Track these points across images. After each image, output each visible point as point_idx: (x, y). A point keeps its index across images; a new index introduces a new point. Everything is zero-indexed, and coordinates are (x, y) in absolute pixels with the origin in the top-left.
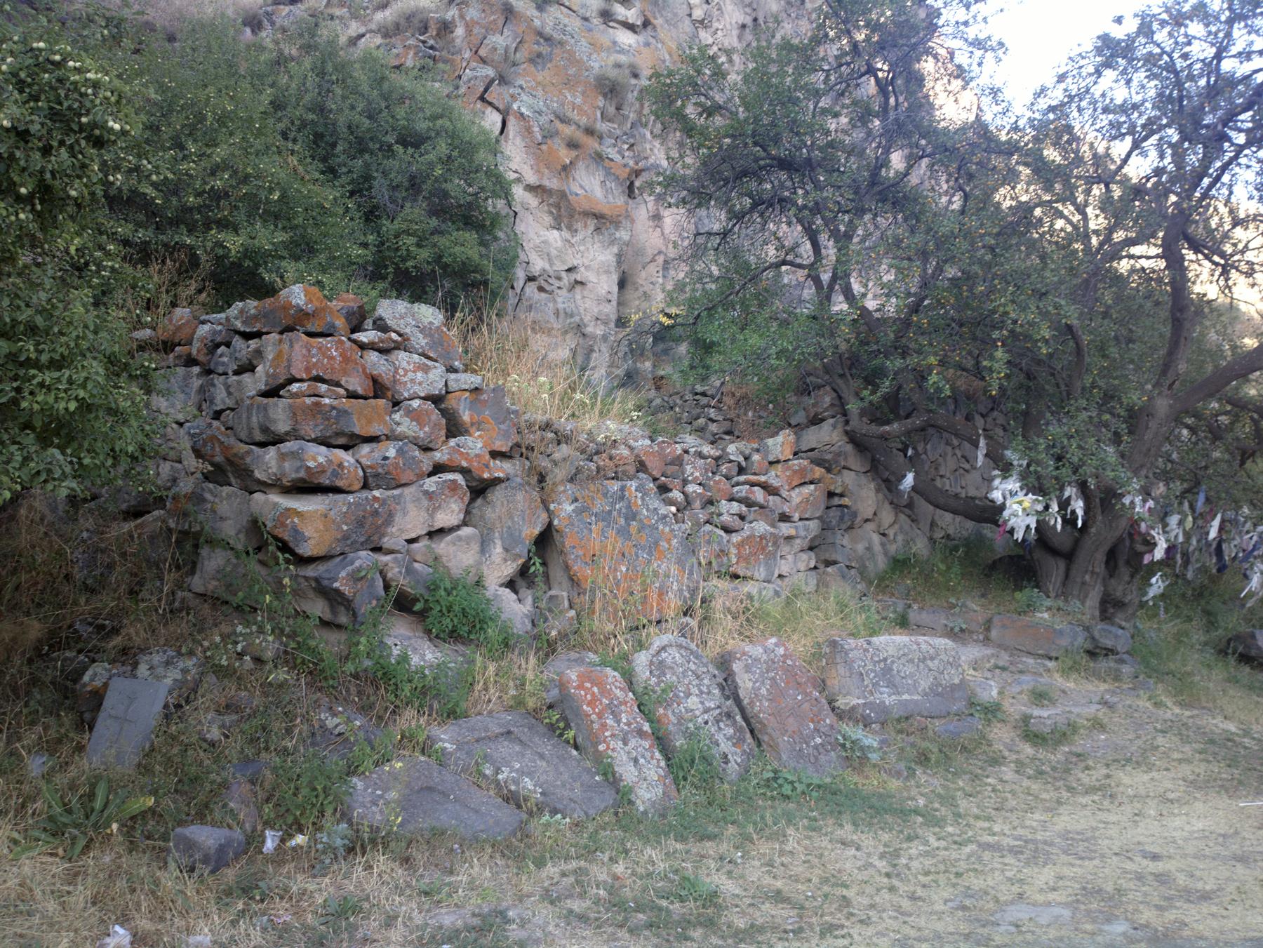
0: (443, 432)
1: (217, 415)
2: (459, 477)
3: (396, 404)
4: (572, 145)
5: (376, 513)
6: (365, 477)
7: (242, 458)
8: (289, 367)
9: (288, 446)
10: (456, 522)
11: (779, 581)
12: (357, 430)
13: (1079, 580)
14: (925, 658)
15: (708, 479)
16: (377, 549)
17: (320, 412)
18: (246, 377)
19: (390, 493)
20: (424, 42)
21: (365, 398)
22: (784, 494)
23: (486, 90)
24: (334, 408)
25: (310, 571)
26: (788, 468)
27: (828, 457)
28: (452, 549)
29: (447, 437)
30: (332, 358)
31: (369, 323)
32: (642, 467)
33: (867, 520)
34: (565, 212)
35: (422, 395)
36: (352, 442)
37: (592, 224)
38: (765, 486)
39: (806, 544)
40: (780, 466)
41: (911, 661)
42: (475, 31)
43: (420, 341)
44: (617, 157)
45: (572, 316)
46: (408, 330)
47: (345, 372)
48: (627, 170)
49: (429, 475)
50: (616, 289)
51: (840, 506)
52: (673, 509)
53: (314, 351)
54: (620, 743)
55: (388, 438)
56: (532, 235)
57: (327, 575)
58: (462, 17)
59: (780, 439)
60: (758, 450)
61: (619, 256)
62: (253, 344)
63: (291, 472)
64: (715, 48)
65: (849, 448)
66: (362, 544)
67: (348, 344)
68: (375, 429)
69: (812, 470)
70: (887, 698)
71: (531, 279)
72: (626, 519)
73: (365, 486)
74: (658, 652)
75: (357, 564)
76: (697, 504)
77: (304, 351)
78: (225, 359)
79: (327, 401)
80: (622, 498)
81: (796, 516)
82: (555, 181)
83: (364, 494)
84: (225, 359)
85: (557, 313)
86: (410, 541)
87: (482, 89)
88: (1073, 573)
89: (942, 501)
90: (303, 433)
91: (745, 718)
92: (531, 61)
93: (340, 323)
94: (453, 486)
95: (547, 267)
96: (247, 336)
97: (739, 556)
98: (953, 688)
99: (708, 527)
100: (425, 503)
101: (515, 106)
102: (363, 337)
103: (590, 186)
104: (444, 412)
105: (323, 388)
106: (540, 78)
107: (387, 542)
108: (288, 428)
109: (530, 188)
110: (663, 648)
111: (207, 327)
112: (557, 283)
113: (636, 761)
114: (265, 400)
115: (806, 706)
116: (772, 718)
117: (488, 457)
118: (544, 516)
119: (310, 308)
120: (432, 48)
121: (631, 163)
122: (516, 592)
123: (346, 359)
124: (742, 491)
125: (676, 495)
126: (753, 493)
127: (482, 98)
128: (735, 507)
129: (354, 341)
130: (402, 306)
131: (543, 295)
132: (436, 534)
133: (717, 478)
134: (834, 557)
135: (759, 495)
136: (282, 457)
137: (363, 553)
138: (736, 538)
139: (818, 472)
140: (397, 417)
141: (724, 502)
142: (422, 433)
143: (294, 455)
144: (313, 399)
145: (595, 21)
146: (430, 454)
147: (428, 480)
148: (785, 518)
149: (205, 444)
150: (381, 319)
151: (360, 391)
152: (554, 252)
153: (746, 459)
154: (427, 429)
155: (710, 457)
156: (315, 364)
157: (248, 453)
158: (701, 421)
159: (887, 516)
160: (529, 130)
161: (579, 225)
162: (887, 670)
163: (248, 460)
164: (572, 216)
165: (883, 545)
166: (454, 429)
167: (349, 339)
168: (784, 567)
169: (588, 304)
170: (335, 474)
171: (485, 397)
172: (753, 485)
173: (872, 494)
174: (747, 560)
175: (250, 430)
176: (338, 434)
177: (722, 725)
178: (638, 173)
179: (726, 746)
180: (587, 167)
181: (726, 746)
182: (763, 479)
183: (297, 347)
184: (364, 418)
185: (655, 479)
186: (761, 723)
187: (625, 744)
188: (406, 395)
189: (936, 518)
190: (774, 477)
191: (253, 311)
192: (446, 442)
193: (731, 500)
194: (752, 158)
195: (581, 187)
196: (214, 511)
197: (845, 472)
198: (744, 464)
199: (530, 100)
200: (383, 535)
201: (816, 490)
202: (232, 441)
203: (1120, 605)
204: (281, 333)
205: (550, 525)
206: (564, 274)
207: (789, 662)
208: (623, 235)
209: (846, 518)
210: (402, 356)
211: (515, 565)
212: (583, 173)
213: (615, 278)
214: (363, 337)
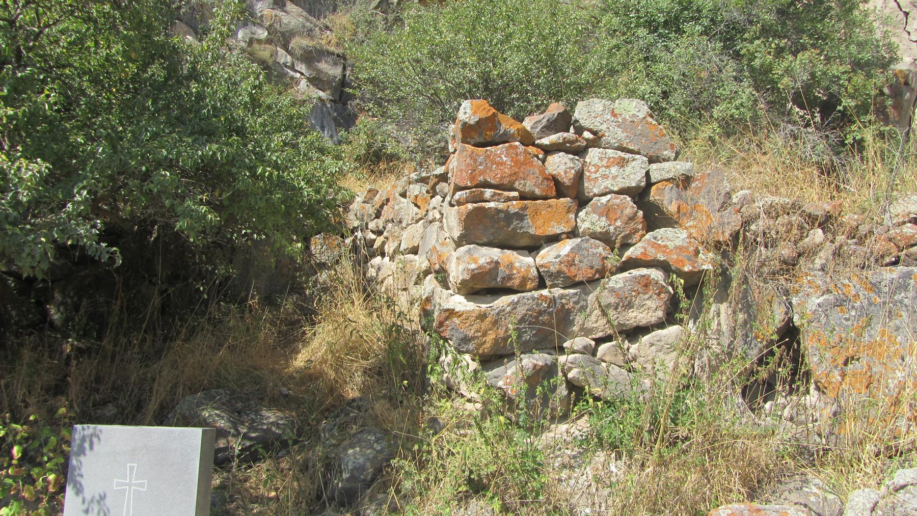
2: (656, 274)
3: (582, 201)
10: (653, 320)
21: (545, 198)
30: (503, 163)
35: (616, 189)
43: (614, 134)
46: (604, 127)
68: (557, 229)
73: (542, 285)
79: (492, 205)
83: (536, 294)
94: (646, 283)
105: (488, 193)
132: (634, 333)
151: (537, 192)
154: (618, 223)
156: (482, 173)
188: (596, 191)
210: (593, 154)
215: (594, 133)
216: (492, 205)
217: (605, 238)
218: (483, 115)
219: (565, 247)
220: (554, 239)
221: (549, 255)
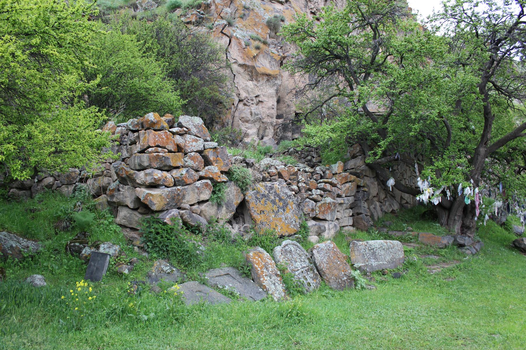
0: (203, 164)
1: (123, 160)
2: (209, 182)
4: (258, 48)
5: (178, 195)
6: (175, 182)
7: (132, 175)
8: (148, 142)
9: (148, 171)
11: (337, 221)
12: (172, 164)
13: (453, 218)
14: (389, 248)
15: (308, 180)
16: (179, 208)
17: (158, 158)
18: (133, 146)
19: (183, 187)
20: (199, 12)
21: (174, 152)
22: (339, 186)
23: (223, 29)
24: (163, 156)
25: (156, 216)
27: (359, 171)
28: (207, 209)
29: (205, 166)
30: (163, 138)
31: (176, 124)
32: (280, 175)
33: (374, 197)
34: (253, 73)
35: (195, 150)
36: (170, 169)
37: (265, 78)
38: (331, 184)
39: (348, 206)
41: (384, 249)
42: (219, 7)
43: (194, 130)
44: (276, 52)
45: (257, 115)
47: (167, 144)
48: (280, 57)
49: (198, 180)
50: (276, 104)
52: (294, 193)
53: (157, 136)
54: (269, 278)
55: (183, 167)
56: (241, 83)
57: (162, 217)
59: (337, 164)
60: (328, 169)
61: (277, 91)
62: (136, 134)
63: (149, 180)
64: (315, 9)
65: (367, 168)
66: (174, 206)
67: (169, 133)
68: (179, 164)
69: (351, 177)
70: (374, 263)
73: (175, 185)
74: (285, 247)
75: (172, 213)
76: (303, 191)
77: (153, 137)
78: (126, 140)
79: (161, 154)
81: (344, 195)
82: (250, 62)
83: (174, 188)
84: (126, 140)
85: (251, 114)
86: (191, 205)
87: (221, 29)
88: (451, 216)
89: (402, 188)
90: (153, 166)
91: (318, 271)
92: (242, 18)
93: (166, 125)
94: (207, 185)
95: (247, 95)
96: (134, 132)
97: (320, 211)
99: (308, 200)
100: (196, 191)
101: (235, 35)
102: (174, 130)
103: (264, 65)
105: (160, 149)
107: (183, 205)
108: (148, 164)
109: (240, 65)
110: (287, 245)
111: (120, 128)
112: (251, 102)
113: (274, 284)
114: (140, 154)
115: (341, 266)
116: (328, 270)
117: (220, 173)
118: (242, 195)
119: (155, 121)
120: (202, 14)
121: (282, 54)
122: (232, 225)
123: (168, 139)
124: (322, 185)
126: (326, 186)
127: (222, 32)
130: (188, 118)
131: (246, 107)
132: (200, 203)
133: (312, 180)
134: (360, 212)
135: (328, 187)
136: (146, 175)
137: (174, 210)
138: (319, 204)
139: (353, 177)
140: (186, 159)
141: (314, 190)
142: (195, 165)
143: (150, 174)
144: (156, 154)
146: (198, 173)
147: (197, 182)
148: (339, 196)
149: (120, 171)
150: (180, 123)
151: (173, 150)
152: (250, 90)
153: (324, 173)
154: (197, 163)
155: (309, 172)
157: (134, 173)
158: (309, 158)
160: (240, 43)
161: (260, 79)
162: (374, 253)
163: (134, 176)
164: (257, 76)
165: (381, 206)
166: (207, 162)
167: (169, 131)
168: (339, 215)
169: (265, 110)
170: (164, 180)
171: (219, 150)
172: (326, 183)
174: (323, 213)
175: (135, 165)
176: (165, 166)
177: (309, 273)
178: (284, 58)
179: (310, 280)
180: (263, 56)
181: (310, 280)
182: (330, 180)
183: (151, 135)
184: (174, 160)
185: (286, 181)
186: (323, 272)
187: (271, 278)
188: (189, 151)
189: (403, 196)
190: (334, 180)
191: (136, 123)
192: (203, 168)
193: (317, 189)
196: (123, 194)
197: (365, 178)
198: (323, 175)
199: (241, 32)
200: (182, 203)
202: (129, 169)
203: (468, 228)
204: (145, 130)
205: (244, 199)
206: (254, 98)
207: (335, 250)
208: (278, 82)
209: (365, 196)
210: (188, 136)
212: (262, 59)
213: (275, 99)
214: (174, 130)
216: (161, 154)
217: (192, 168)
219: (184, 171)
220: (178, 168)
221: (175, 173)
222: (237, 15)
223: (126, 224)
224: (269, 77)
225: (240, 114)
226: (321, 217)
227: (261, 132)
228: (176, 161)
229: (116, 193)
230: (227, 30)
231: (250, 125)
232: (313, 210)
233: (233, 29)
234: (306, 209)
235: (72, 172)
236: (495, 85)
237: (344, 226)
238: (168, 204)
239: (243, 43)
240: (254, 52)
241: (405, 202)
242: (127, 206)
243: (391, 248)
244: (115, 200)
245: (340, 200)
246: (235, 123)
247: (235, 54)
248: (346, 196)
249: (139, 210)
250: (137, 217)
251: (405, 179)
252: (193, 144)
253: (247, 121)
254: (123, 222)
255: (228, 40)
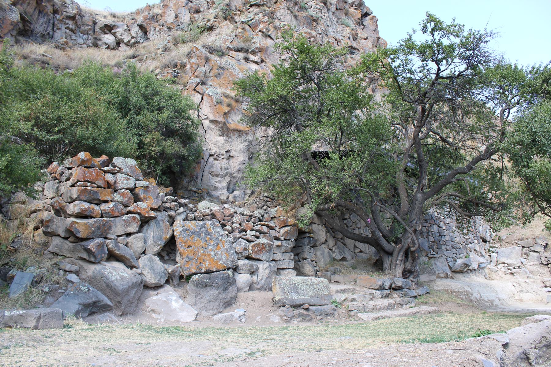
2: (137, 216)
3: (116, 191)
6: (102, 214)
10: (135, 231)
12: (100, 198)
18: (68, 182)
20: (175, 71)
22: (277, 229)
24: (91, 190)
25: (83, 243)
26: (279, 220)
30: (93, 175)
33: (323, 243)
34: (225, 130)
36: (99, 203)
37: (237, 134)
38: (268, 226)
40: (275, 219)
45: (227, 169)
46: (122, 167)
47: (97, 179)
51: (309, 237)
52: (227, 232)
55: (112, 201)
58: (189, 62)
62: (70, 171)
63: (77, 210)
66: (100, 235)
67: (99, 170)
68: (107, 198)
71: (211, 155)
72: (205, 234)
73: (102, 217)
79: (89, 188)
80: (204, 227)
81: (282, 238)
82: (221, 118)
86: (118, 236)
89: (349, 235)
90: (81, 198)
92: (216, 76)
94: (134, 219)
95: (218, 151)
98: (325, 296)
101: (207, 92)
103: (235, 120)
104: (133, 194)
105: (88, 184)
106: (218, 81)
107: (109, 236)
109: (211, 121)
112: (222, 157)
119: (86, 159)
120: (178, 73)
125: (228, 227)
127: (194, 90)
128: (254, 233)
129: (102, 170)
131: (216, 161)
132: (129, 235)
135: (265, 229)
136: (75, 206)
138: (252, 244)
140: (115, 195)
142: (125, 200)
145: (242, 61)
148: (277, 239)
151: (102, 186)
152: (221, 145)
156: (86, 177)
158: (265, 207)
159: (331, 242)
160: (211, 100)
161: (231, 135)
165: (329, 253)
166: (137, 199)
169: (235, 165)
171: (150, 189)
172: (263, 225)
173: (324, 233)
174: (256, 252)
176: (94, 199)
182: (267, 223)
185: (220, 222)
190: (272, 224)
193: (253, 230)
194: (278, 109)
195: (233, 120)
196: (56, 225)
198: (261, 218)
200: (108, 233)
201: (291, 229)
206: (224, 153)
209: (312, 242)
210: (119, 175)
211: (158, 248)
215: (119, 168)
216: (89, 188)
217: (122, 203)
218: (88, 158)
219: (111, 205)
220: (106, 202)
221: (104, 206)
222: (211, 74)
223: (58, 251)
224: (240, 132)
225: (209, 168)
226: (253, 256)
227: (232, 187)
228: (105, 195)
229: (50, 224)
230: (199, 88)
231: (219, 179)
232: (245, 249)
233: (207, 87)
234: (239, 249)
235: (19, 207)
236: (441, 137)
237: (283, 269)
238: (94, 232)
239: (214, 100)
240: (226, 110)
241: (359, 250)
242: (59, 235)
243: (316, 285)
244: (49, 230)
245: (277, 243)
246: (204, 177)
247: (206, 110)
248: (285, 240)
249: (69, 239)
250: (68, 245)
251: (359, 228)
252: (123, 182)
253: (217, 176)
254: (55, 250)
255: (200, 96)
